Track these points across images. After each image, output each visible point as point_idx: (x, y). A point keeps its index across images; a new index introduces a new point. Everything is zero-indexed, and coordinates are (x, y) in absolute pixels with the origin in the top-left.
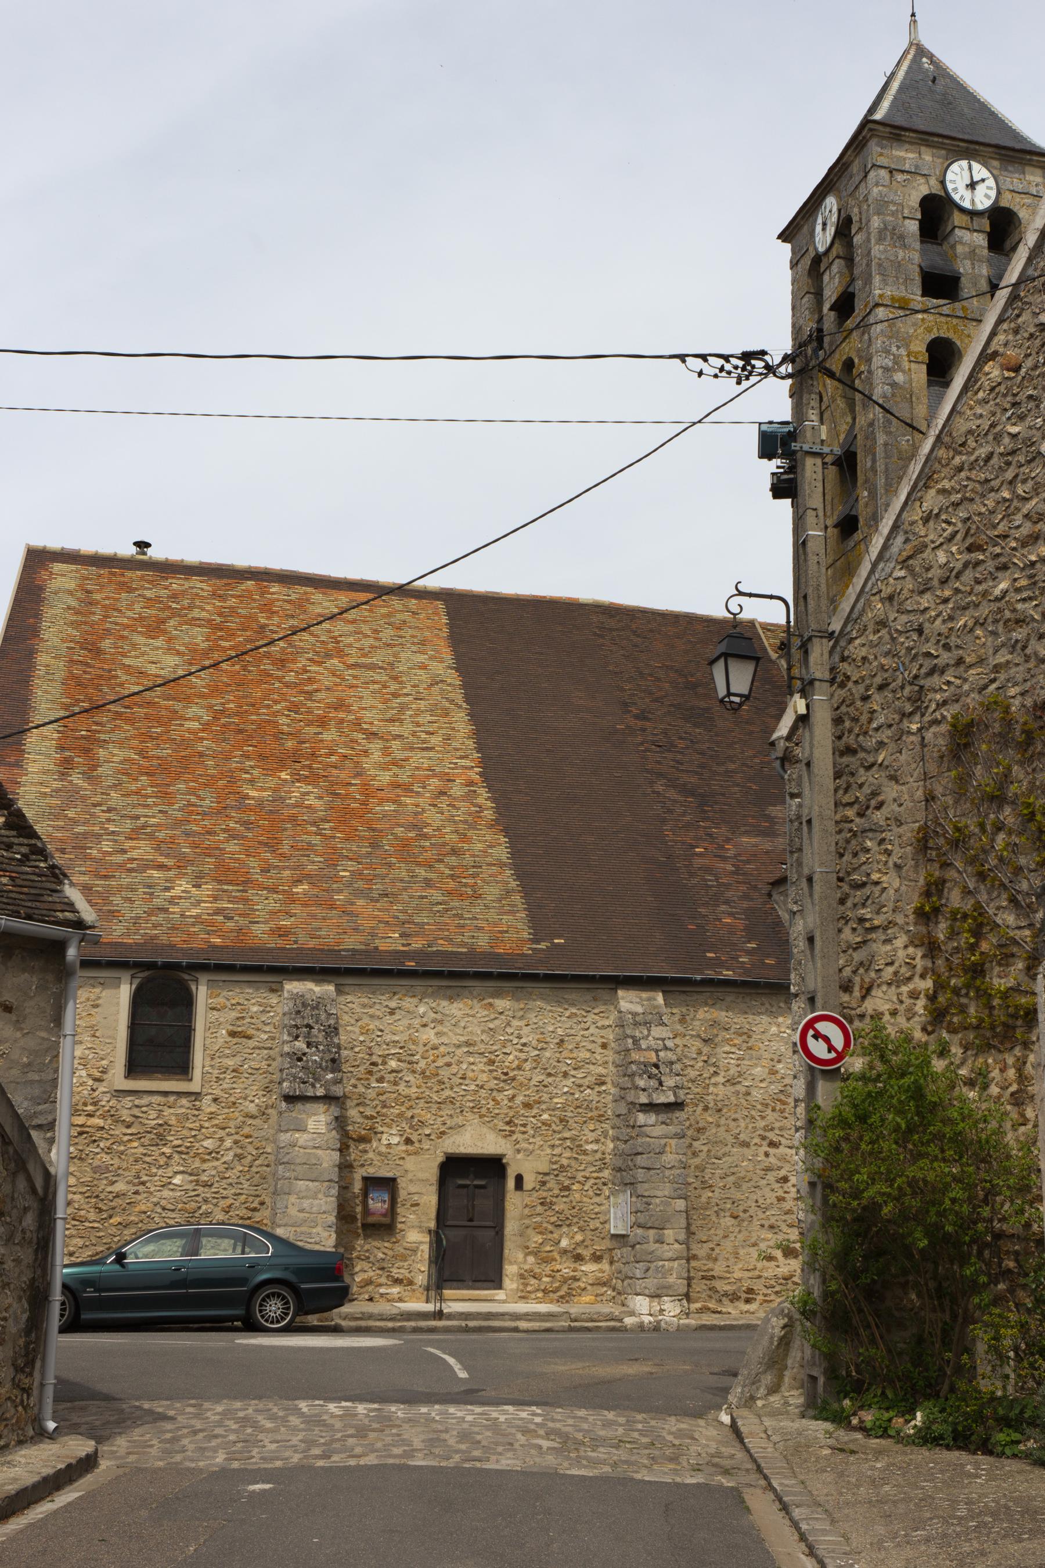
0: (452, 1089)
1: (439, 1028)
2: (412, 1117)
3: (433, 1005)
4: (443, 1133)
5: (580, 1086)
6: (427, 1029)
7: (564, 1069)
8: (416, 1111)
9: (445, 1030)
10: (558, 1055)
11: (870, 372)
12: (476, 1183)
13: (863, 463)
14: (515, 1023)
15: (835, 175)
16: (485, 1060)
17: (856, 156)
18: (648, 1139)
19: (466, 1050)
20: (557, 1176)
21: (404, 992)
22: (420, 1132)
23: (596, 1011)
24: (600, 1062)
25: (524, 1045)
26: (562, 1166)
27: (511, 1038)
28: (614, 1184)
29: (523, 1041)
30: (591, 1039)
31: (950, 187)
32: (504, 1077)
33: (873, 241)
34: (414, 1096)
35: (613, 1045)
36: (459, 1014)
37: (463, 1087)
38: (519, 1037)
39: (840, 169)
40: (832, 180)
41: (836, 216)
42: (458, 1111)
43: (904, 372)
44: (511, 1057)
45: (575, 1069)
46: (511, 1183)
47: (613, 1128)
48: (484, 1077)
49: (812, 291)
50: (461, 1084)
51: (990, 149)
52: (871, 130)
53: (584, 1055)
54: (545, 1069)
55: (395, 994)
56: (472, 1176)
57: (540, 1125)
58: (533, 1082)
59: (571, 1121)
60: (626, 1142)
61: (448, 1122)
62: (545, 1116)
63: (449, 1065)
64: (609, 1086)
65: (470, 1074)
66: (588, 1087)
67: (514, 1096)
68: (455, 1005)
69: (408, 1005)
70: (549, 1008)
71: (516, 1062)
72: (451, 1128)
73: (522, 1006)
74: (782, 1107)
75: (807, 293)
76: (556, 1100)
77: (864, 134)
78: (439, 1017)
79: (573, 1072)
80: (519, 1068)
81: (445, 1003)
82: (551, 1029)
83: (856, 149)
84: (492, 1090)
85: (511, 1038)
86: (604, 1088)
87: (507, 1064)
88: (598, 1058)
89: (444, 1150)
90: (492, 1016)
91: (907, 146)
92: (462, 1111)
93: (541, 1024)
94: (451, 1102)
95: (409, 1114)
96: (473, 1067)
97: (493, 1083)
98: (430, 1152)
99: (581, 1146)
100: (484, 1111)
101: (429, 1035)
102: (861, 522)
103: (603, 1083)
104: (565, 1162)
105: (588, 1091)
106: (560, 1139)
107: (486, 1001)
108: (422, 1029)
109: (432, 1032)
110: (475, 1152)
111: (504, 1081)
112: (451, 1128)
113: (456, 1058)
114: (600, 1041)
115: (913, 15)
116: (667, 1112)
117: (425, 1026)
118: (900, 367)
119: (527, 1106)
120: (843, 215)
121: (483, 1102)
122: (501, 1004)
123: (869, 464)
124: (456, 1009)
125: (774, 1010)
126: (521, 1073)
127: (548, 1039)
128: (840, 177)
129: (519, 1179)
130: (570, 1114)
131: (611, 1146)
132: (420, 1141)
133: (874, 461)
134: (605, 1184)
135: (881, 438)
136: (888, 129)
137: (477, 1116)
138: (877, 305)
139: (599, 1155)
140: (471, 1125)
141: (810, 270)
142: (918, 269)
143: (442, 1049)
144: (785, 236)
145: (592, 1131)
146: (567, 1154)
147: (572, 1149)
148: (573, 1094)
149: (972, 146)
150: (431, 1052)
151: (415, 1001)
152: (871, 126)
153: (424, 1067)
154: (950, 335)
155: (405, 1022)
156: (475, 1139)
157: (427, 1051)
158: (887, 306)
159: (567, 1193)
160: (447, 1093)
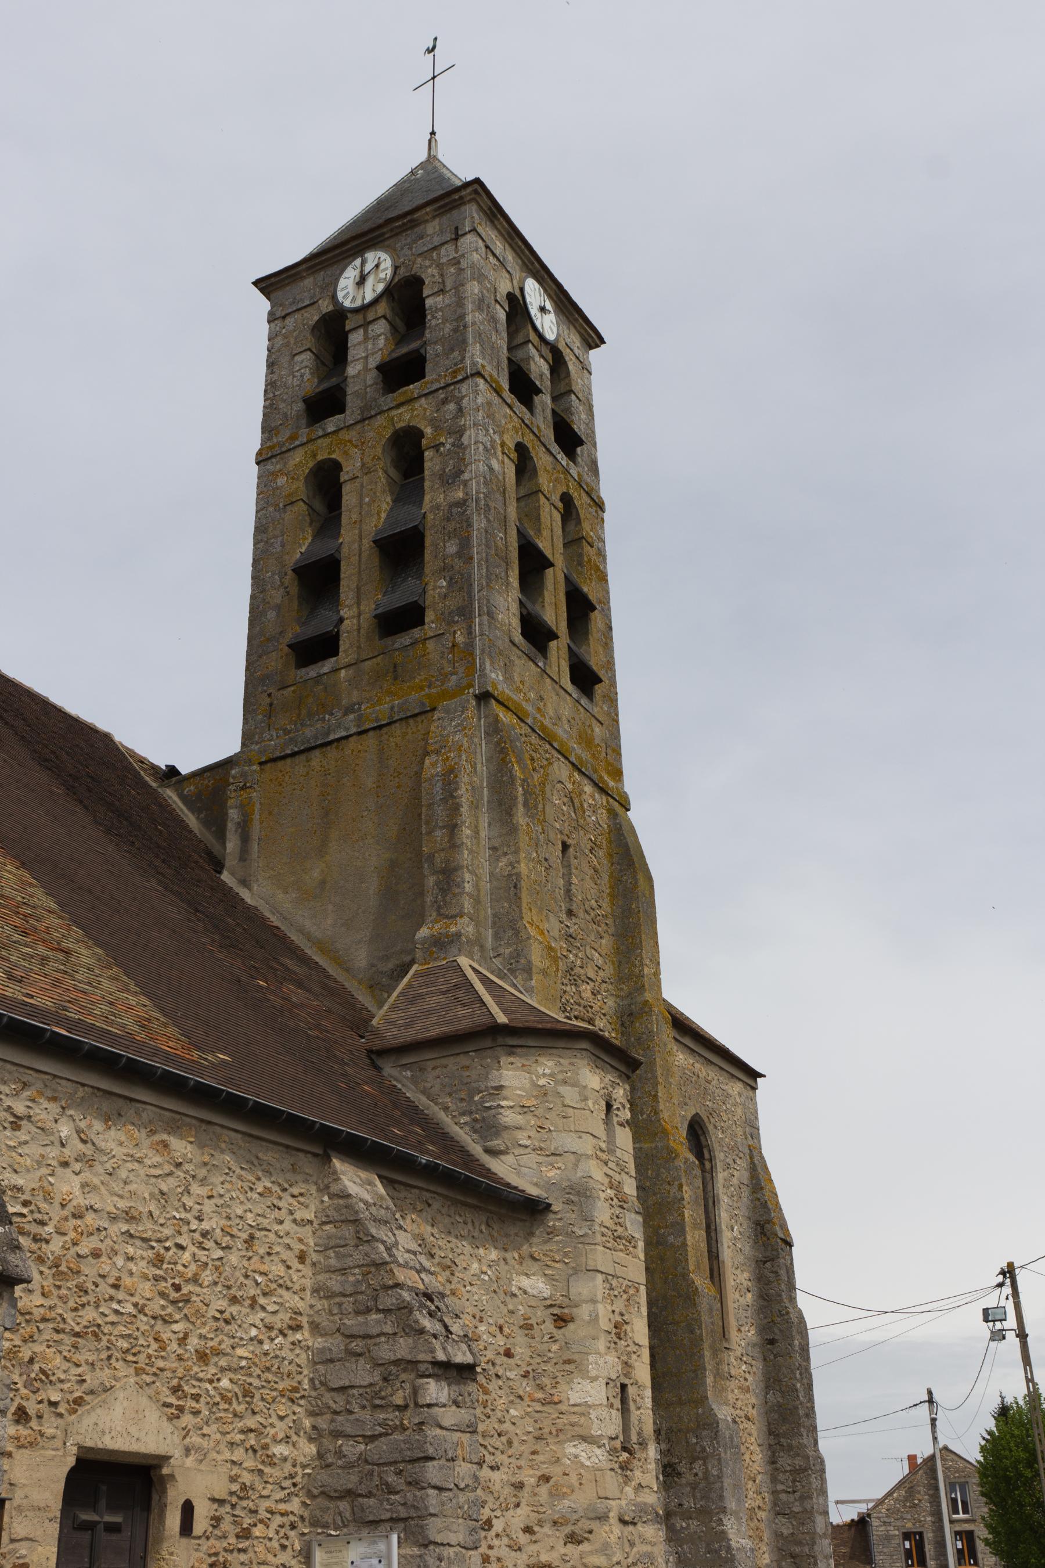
0: (97, 1307)
1: (86, 1176)
2: (31, 1361)
3: (83, 1125)
4: (79, 1401)
5: (270, 1328)
6: (68, 1171)
7: (252, 1292)
8: (39, 1348)
9: (96, 1181)
10: (245, 1263)
11: (459, 446)
12: (109, 1518)
13: (439, 547)
14: (196, 1189)
15: (392, 230)
16: (150, 1253)
17: (434, 217)
18: (438, 1431)
19: (124, 1228)
20: (233, 1506)
21: (39, 1085)
22: (42, 1395)
23: (295, 1191)
24: (297, 1287)
25: (205, 1234)
26: (244, 1487)
27: (188, 1216)
28: (314, 1524)
29: (205, 1226)
30: (287, 1241)
31: (528, 299)
32: (173, 1295)
33: (470, 307)
34: (38, 1313)
35: (315, 1257)
36: (119, 1151)
37: (115, 1306)
38: (200, 1219)
39: (404, 224)
40: (383, 234)
41: (389, 272)
42: (104, 1355)
43: (498, 459)
44: (187, 1256)
45: (265, 1294)
46: (173, 1520)
47: (312, 1414)
48: (146, 1289)
49: (314, 350)
50: (111, 1298)
51: (554, 287)
52: (476, 192)
53: (277, 1269)
54: (229, 1288)
55: (25, 1085)
56: (103, 1503)
57: (218, 1399)
58: (212, 1312)
59: (257, 1396)
60: (373, 1438)
61: (87, 1377)
62: (225, 1383)
63: (96, 1254)
64: (307, 1334)
65: (127, 1281)
66: (281, 1332)
67: (186, 1336)
68: (112, 1132)
69: (44, 1116)
70: (238, 1171)
71: (193, 1267)
72: (92, 1392)
73: (206, 1158)
74: (486, 1397)
75: (309, 349)
76: (240, 1352)
77: (463, 193)
78: (88, 1150)
79: (262, 1301)
80: (195, 1280)
81: (98, 1125)
82: (239, 1212)
83: (440, 208)
84: (154, 1318)
85: (188, 1216)
86: (299, 1336)
87: (180, 1268)
88: (295, 1278)
89: (79, 1439)
90: (168, 1168)
91: (496, 232)
92: (109, 1357)
93: (227, 1198)
94: (95, 1334)
95: (26, 1354)
96: (131, 1265)
97: (156, 1305)
98: (58, 1443)
99: (266, 1447)
100: (142, 1358)
101: (68, 1185)
102: (430, 616)
103: (298, 1328)
104: (247, 1478)
105: (280, 1339)
106: (242, 1432)
107: (157, 1138)
108: (59, 1170)
109: (77, 1181)
110: (135, 1447)
111: (174, 1302)
112: (92, 1392)
113: (108, 1241)
114: (298, 1247)
115: (433, 133)
116: (458, 1383)
117: (65, 1164)
118: (495, 453)
119: (203, 1357)
120: (402, 272)
121: (141, 1341)
122: (181, 1147)
123: (452, 548)
124: (113, 1140)
125: (476, 1234)
126: (198, 1289)
127: (235, 1232)
128: (397, 234)
129: (188, 1509)
130: (256, 1382)
131: (312, 1449)
132: (40, 1417)
133: (465, 544)
134: (293, 1527)
135: (479, 523)
136: (489, 203)
137: (132, 1371)
138: (479, 374)
139: (288, 1468)
140: (124, 1388)
141: (315, 328)
142: (506, 362)
143: (90, 1218)
144: (266, 285)
145: (281, 1418)
146: (250, 1463)
147: (255, 1451)
148: (261, 1342)
149: (543, 272)
150: (73, 1222)
151: (54, 1108)
152: (476, 186)
153: (58, 1252)
154: (529, 445)
155: (34, 1150)
156: (127, 1423)
157: (66, 1219)
158: (486, 380)
159: (247, 1543)
160: (89, 1314)
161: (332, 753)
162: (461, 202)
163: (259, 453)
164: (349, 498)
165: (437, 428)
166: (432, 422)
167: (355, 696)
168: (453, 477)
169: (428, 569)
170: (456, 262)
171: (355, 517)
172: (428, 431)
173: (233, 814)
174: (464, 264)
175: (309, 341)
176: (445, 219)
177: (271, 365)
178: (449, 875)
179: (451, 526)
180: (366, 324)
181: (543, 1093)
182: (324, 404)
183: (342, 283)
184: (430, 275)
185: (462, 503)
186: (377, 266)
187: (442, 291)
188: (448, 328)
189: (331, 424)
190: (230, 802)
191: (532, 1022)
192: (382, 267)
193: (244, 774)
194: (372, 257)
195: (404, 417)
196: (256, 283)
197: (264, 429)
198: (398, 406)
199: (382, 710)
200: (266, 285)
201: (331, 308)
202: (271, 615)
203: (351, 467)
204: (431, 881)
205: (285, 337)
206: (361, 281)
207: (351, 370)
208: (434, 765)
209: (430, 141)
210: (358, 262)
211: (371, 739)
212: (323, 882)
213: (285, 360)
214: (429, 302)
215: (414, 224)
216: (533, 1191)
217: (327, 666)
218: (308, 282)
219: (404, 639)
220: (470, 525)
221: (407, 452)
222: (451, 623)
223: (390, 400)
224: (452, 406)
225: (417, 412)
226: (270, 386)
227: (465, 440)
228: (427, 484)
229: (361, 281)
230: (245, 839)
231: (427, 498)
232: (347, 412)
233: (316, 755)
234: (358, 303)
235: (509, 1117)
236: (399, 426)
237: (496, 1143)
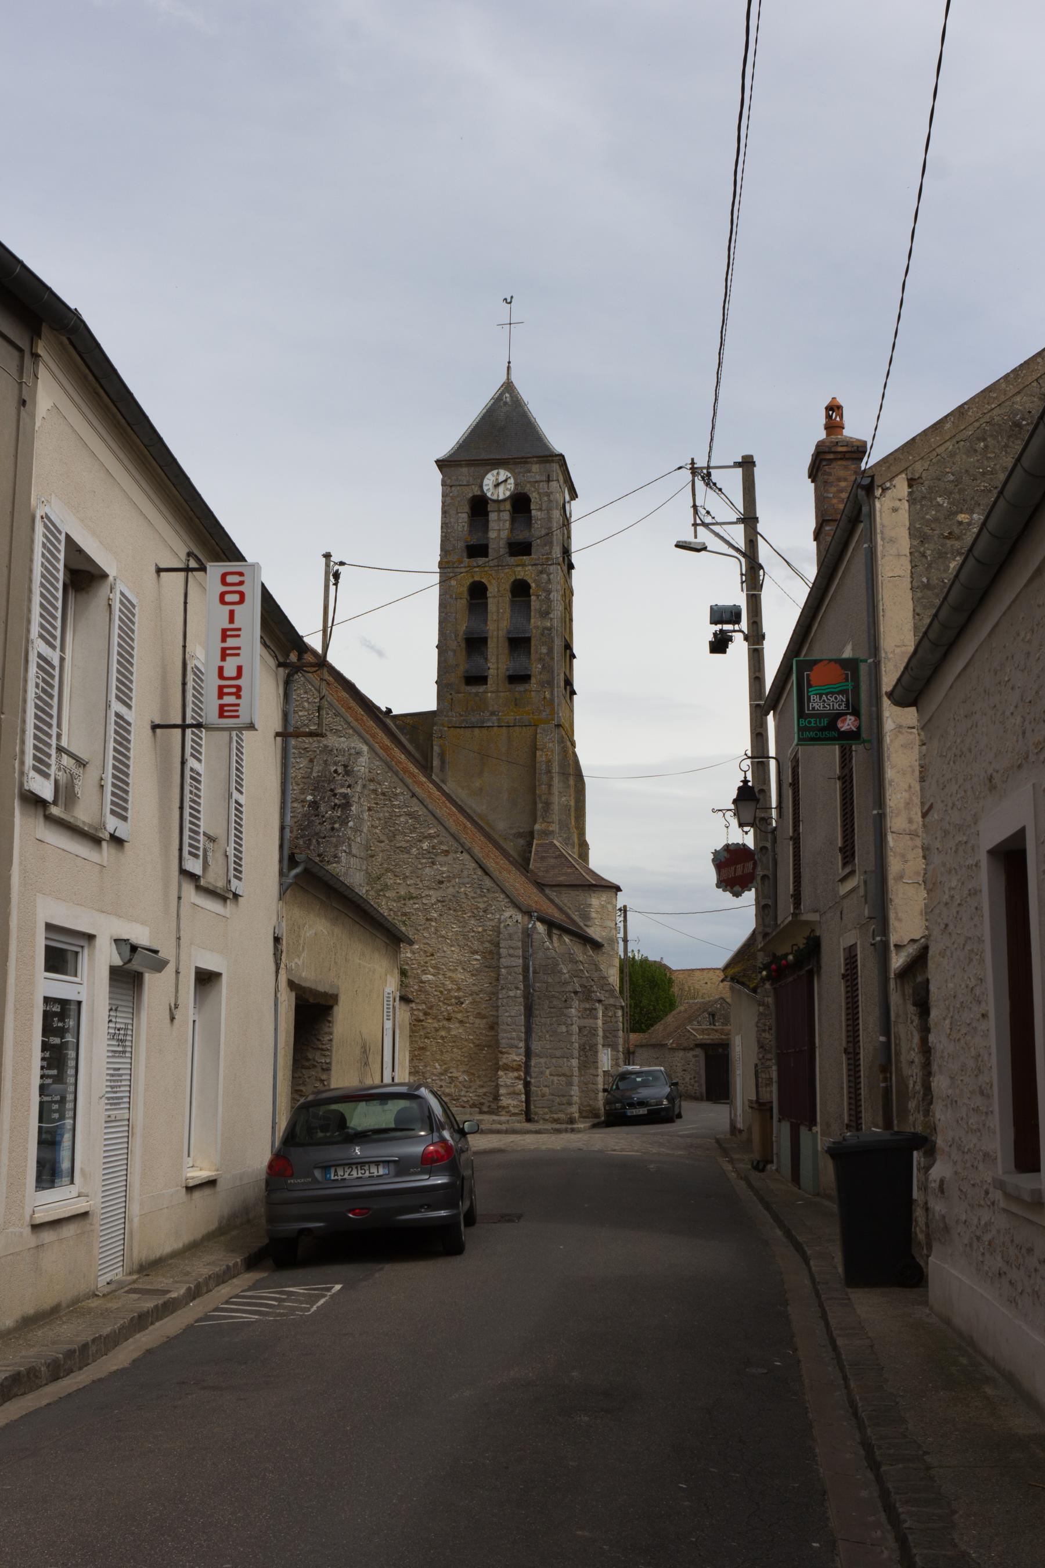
11: (548, 600)
13: (538, 648)
41: (513, 486)
102: (533, 680)
120: (520, 490)
123: (544, 650)
133: (551, 650)
161: (484, 731)
162: (552, 461)
163: (440, 563)
164: (492, 606)
165: (537, 586)
166: (535, 581)
167: (496, 708)
168: (545, 614)
169: (533, 656)
170: (548, 495)
171: (495, 618)
172: (533, 585)
173: (436, 748)
174: (552, 498)
175: (467, 509)
176: (542, 466)
177: (444, 512)
178: (548, 805)
179: (544, 639)
180: (499, 511)
181: (603, 907)
182: (477, 550)
183: (486, 482)
184: (534, 496)
185: (550, 629)
186: (506, 481)
187: (540, 509)
188: (543, 532)
189: (481, 561)
190: (434, 743)
191: (603, 883)
192: (509, 481)
193: (440, 731)
194: (503, 474)
195: (521, 573)
196: (437, 462)
197: (442, 549)
198: (517, 566)
199: (510, 718)
200: (441, 464)
201: (479, 493)
202: (450, 653)
203: (492, 590)
204: (540, 806)
205: (452, 498)
206: (497, 485)
207: (492, 535)
208: (541, 756)
209: (509, 368)
210: (495, 472)
211: (504, 730)
212: (481, 789)
213: (453, 512)
214: (533, 513)
215: (526, 463)
216: (600, 940)
217: (481, 689)
218: (465, 470)
219: (521, 688)
220: (553, 641)
221: (521, 590)
222: (543, 686)
223: (513, 560)
224: (545, 576)
225: (526, 571)
226: (444, 525)
227: (551, 596)
228: (532, 613)
229: (497, 485)
230: (443, 762)
231: (532, 621)
232: (490, 558)
233: (477, 731)
234: (495, 497)
235: (593, 915)
236: (519, 577)
237: (589, 923)
